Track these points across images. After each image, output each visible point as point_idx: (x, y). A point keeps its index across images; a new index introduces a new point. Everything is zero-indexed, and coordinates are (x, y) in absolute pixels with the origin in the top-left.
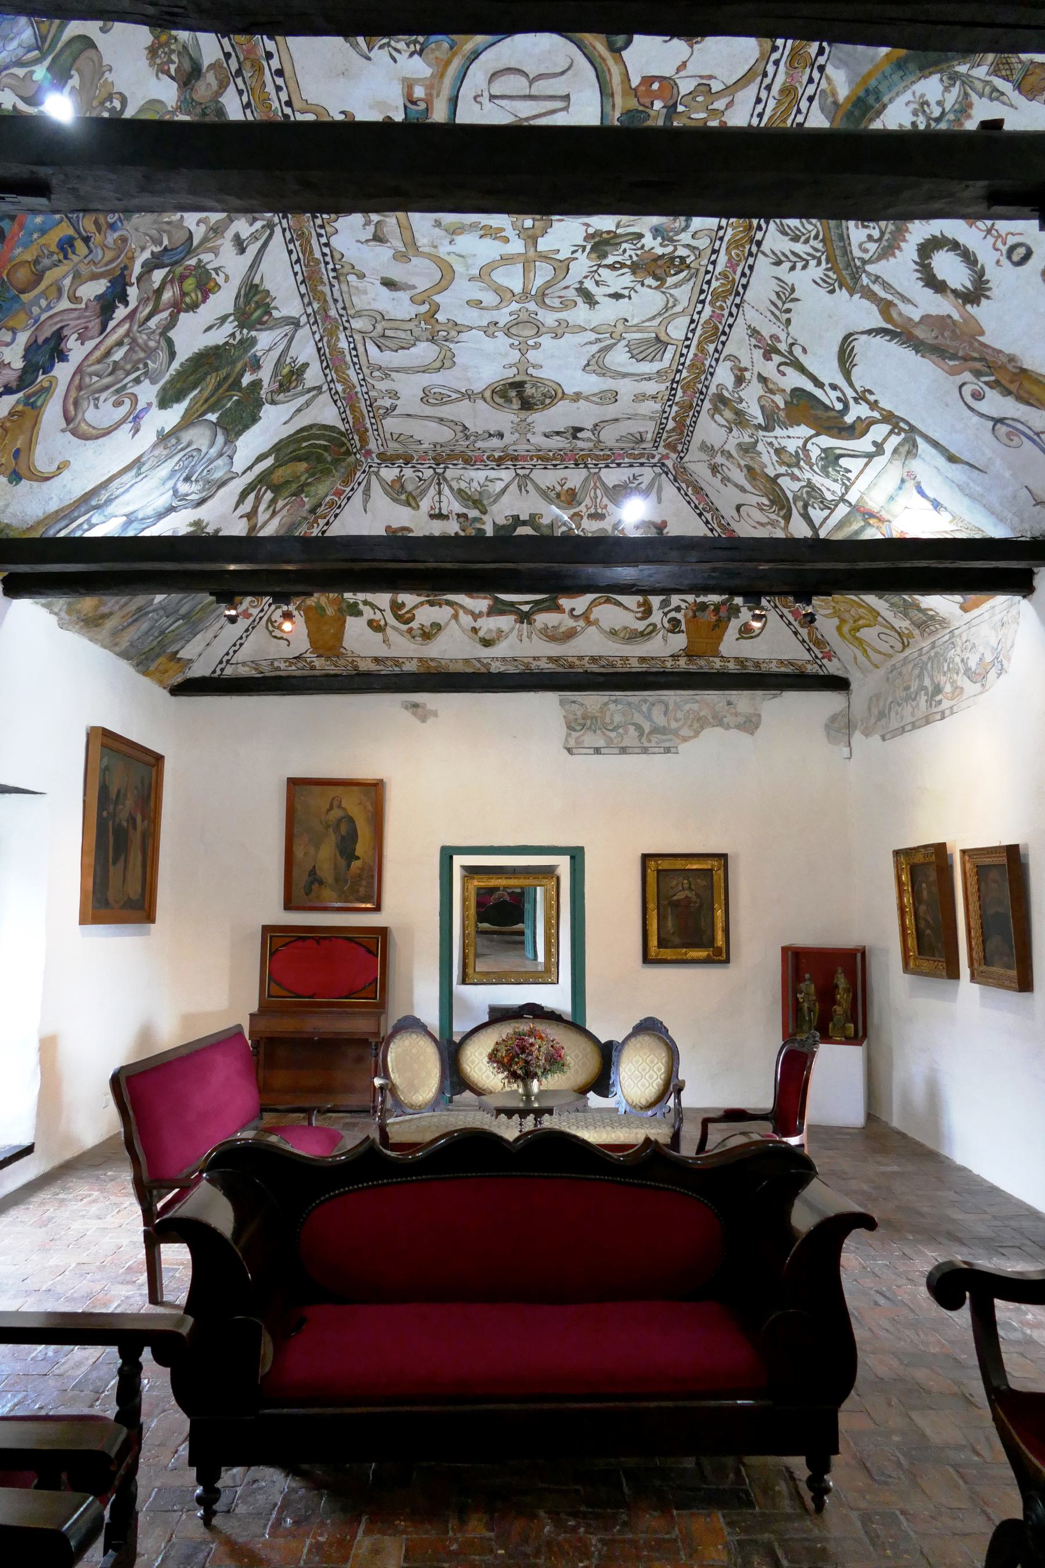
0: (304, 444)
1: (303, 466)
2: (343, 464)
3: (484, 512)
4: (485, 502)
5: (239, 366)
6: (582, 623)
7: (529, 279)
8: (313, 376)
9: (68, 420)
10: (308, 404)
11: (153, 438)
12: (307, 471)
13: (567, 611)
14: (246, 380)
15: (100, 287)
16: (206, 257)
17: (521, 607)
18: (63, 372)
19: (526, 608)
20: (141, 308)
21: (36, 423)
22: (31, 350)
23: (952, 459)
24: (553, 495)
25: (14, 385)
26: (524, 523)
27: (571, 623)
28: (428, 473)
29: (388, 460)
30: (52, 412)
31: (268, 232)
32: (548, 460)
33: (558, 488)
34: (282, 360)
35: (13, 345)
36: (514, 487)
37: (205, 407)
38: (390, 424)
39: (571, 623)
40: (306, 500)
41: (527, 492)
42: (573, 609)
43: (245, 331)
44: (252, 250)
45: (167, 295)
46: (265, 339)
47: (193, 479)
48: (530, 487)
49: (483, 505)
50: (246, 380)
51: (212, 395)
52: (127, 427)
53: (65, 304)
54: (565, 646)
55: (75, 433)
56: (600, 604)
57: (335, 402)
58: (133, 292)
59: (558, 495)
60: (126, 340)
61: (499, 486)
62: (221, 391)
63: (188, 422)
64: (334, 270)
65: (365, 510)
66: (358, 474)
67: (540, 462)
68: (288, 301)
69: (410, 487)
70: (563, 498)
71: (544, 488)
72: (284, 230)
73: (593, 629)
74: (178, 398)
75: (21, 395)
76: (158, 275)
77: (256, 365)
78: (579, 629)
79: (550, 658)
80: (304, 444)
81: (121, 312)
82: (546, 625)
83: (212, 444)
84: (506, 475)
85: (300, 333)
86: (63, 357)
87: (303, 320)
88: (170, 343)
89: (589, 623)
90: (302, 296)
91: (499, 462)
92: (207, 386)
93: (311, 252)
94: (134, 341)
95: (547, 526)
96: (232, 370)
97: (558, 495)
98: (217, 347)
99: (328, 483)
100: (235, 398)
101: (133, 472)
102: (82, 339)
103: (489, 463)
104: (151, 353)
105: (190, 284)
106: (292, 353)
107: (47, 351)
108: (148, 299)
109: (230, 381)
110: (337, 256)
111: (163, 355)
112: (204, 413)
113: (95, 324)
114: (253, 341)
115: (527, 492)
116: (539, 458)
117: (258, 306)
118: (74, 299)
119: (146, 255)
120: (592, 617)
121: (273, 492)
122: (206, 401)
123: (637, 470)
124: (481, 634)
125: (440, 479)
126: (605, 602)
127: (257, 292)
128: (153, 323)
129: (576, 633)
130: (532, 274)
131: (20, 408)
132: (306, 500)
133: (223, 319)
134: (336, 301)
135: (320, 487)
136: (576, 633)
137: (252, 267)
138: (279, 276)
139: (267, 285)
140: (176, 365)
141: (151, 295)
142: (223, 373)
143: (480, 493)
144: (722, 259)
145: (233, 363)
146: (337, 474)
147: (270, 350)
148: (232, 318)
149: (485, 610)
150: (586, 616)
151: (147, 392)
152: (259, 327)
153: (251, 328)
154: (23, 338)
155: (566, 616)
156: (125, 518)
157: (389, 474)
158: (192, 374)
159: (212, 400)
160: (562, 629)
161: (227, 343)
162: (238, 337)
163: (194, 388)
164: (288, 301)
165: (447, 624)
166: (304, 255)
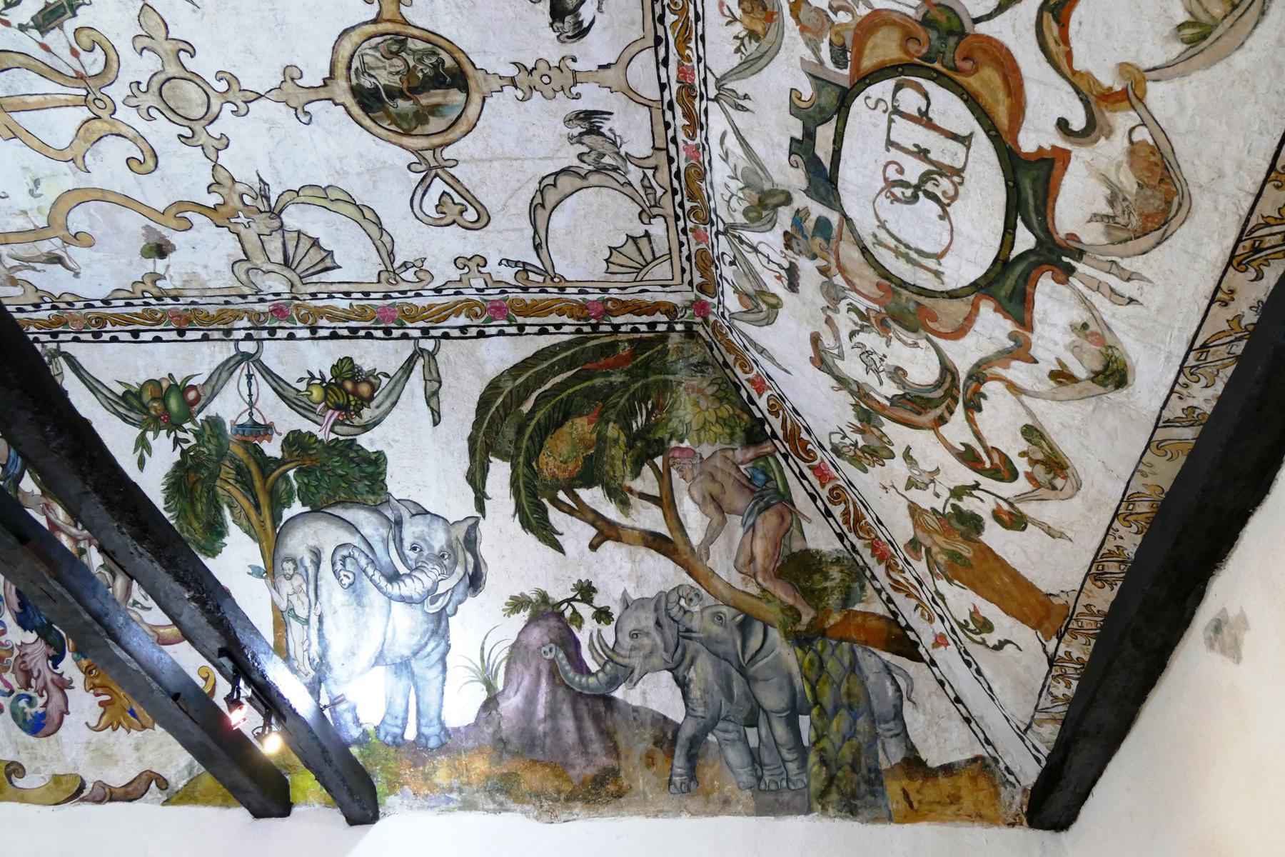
0: (526, 408)
1: (581, 426)
2: (671, 358)
3: (788, 200)
4: (767, 186)
5: (237, 450)
6: (1123, 120)
7: (41, 103)
8: (377, 356)
11: (261, 585)
12: (602, 420)
13: (1061, 143)
14: (272, 449)
17: (1019, 248)
19: (1025, 240)
20: (52, 517)
24: (752, 47)
25: (52, 652)
26: (809, 135)
27: (1112, 149)
31: (61, 359)
32: (686, 27)
33: (738, 28)
34: (291, 394)
35: (9, 629)
36: (737, 116)
37: (266, 512)
39: (1112, 149)
40: (686, 444)
41: (746, 97)
42: (1063, 125)
43: (187, 426)
47: (402, 569)
48: (740, 86)
49: (773, 193)
50: (272, 449)
51: (255, 497)
54: (1201, 202)
56: (1064, 39)
57: (481, 335)
59: (753, 35)
60: (82, 545)
62: (258, 484)
64: (158, 299)
65: (786, 371)
66: (730, 337)
67: (692, 45)
68: (193, 360)
70: (759, 28)
71: (736, 60)
72: (76, 340)
73: (1158, 95)
75: (68, 655)
77: (266, 430)
78: (1142, 135)
79: (1234, 261)
80: (526, 408)
82: (1095, 217)
83: (352, 527)
84: (717, 122)
87: (248, 347)
89: (1130, 93)
90: (206, 338)
91: (696, 124)
92: (231, 495)
93: (136, 315)
95: (818, 90)
96: (233, 459)
97: (753, 35)
98: (179, 465)
99: (684, 397)
100: (291, 473)
101: (295, 627)
103: (698, 140)
106: (291, 374)
108: (47, 505)
109: (253, 468)
110: (127, 295)
112: (276, 517)
114: (215, 423)
115: (746, 97)
116: (683, 41)
117: (163, 399)
120: (1108, 79)
121: (589, 485)
122: (257, 507)
124: (1080, 372)
126: (1063, 25)
127: (138, 396)
129: (1156, 149)
130: (30, 99)
131: (85, 663)
132: (686, 444)
133: (142, 443)
134: (227, 303)
135: (681, 413)
136: (1156, 149)
137: (93, 390)
139: (137, 378)
141: (44, 500)
142: (227, 471)
143: (747, 186)
145: (222, 453)
146: (678, 377)
147: (251, 405)
148: (150, 435)
149: (1009, 325)
150: (1097, 100)
152: (197, 407)
153: (190, 417)
155: (1081, 156)
156: (380, 669)
158: (192, 504)
159: (263, 499)
160: (1128, 182)
161: (183, 453)
162: (190, 436)
163: (219, 510)
164: (193, 360)
165: (1030, 413)
166: (134, 323)
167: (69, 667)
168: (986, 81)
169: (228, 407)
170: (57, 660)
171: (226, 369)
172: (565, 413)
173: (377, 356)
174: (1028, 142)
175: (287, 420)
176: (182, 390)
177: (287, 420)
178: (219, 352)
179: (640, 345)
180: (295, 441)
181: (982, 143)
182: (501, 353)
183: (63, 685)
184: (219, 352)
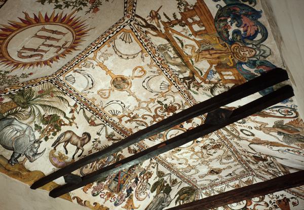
1: (186, 195)
8: (179, 180)
9: (137, 199)
10: (180, 184)
14: (165, 184)
15: (134, 180)
16: (148, 171)
18: (133, 192)
21: (132, 201)
22: (127, 191)
23: (282, 159)
28: (210, 189)
29: (203, 189)
30: (134, 198)
36: (226, 187)
38: (198, 183)
44: (156, 167)
45: (145, 177)
46: (165, 178)
50: (165, 184)
52: (148, 197)
53: (130, 183)
55: (139, 200)
58: (139, 179)
61: (224, 188)
63: (158, 193)
68: (167, 171)
69: (208, 193)
74: (154, 190)
76: (142, 176)
77: (166, 182)
81: (139, 182)
84: (224, 185)
85: (172, 175)
86: (133, 190)
88: (149, 184)
91: (222, 183)
94: (143, 185)
102: (134, 187)
104: (146, 186)
105: (148, 175)
106: (172, 178)
107: (130, 190)
111: (148, 185)
113: (136, 185)
114: (163, 179)
118: (131, 182)
119: (139, 174)
123: (249, 177)
125: (213, 190)
128: (144, 182)
133: (156, 177)
138: (162, 168)
139: (161, 171)
140: (151, 186)
144: (226, 142)
145: (161, 183)
151: (148, 191)
153: (162, 177)
154: (126, 190)
157: (204, 191)
164: (167, 171)
167: (127, 199)
168: (249, 203)
169: (165, 178)
170: (126, 197)
171: (168, 174)
172: (185, 193)
173: (179, 180)
174: (247, 207)
175: (168, 182)
176: (163, 174)
177: (168, 182)
178: (169, 172)
179: (194, 190)
180: (168, 185)
181: (244, 205)
182: (186, 185)
183: (124, 201)
184: (169, 172)
